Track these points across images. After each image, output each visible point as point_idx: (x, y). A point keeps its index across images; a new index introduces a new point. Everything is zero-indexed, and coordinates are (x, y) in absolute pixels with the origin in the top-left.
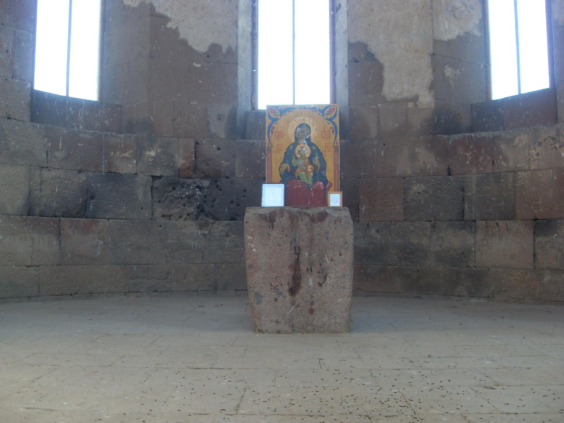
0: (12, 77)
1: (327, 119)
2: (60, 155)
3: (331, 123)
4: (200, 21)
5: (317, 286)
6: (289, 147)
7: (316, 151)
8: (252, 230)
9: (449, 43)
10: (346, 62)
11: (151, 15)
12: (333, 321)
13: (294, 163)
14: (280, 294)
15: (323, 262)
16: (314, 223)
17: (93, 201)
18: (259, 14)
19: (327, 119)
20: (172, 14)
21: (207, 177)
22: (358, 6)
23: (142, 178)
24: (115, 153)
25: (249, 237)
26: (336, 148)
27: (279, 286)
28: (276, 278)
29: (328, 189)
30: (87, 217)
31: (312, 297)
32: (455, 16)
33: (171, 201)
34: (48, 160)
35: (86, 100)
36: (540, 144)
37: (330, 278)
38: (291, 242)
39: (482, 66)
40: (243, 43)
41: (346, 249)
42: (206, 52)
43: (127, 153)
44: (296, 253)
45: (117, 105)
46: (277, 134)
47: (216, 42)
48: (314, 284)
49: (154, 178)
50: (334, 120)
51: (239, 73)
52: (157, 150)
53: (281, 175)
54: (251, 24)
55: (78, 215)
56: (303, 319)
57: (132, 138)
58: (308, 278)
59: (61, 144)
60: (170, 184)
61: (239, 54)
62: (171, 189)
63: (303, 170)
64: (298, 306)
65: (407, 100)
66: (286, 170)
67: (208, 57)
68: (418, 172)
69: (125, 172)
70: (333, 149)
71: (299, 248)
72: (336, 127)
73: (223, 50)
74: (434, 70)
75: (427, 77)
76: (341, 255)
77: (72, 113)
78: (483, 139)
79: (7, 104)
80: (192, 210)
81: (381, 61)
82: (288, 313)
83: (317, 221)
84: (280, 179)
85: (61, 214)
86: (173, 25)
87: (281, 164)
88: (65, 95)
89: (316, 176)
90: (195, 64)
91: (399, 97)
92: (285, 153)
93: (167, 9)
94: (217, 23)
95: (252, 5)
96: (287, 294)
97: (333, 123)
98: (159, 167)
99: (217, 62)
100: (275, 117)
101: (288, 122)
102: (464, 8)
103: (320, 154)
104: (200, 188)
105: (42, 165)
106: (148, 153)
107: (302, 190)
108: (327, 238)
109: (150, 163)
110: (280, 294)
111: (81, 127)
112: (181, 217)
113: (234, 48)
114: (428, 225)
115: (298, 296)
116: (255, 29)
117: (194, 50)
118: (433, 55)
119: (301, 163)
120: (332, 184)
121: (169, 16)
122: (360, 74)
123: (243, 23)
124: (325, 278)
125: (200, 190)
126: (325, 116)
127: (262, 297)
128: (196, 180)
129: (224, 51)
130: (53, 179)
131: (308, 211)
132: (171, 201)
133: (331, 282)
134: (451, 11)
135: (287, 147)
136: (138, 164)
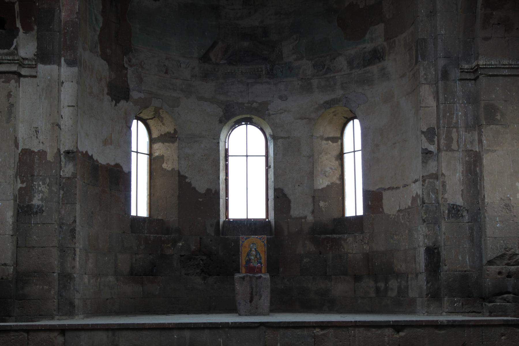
0: (125, 214)
1: (262, 241)
2: (142, 247)
4: (201, 177)
6: (248, 252)
9: (323, 189)
10: (273, 197)
12: (264, 311)
19: (262, 241)
22: (279, 170)
25: (237, 284)
26: (265, 252)
32: (326, 176)
36: (357, 242)
39: (340, 198)
40: (222, 186)
42: (204, 193)
49: (181, 256)
53: (245, 262)
54: (225, 174)
65: (301, 218)
66: (247, 260)
67: (205, 195)
70: (264, 252)
72: (265, 244)
75: (311, 208)
76: (266, 290)
77: (142, 225)
78: (334, 238)
80: (198, 271)
81: (290, 198)
90: (199, 199)
91: (298, 216)
96: (249, 302)
100: (243, 241)
102: (331, 171)
106: (178, 244)
108: (262, 284)
110: (247, 302)
112: (193, 274)
113: (218, 191)
121: (187, 176)
124: (261, 297)
125: (202, 261)
129: (213, 192)
131: (255, 275)
134: (324, 174)
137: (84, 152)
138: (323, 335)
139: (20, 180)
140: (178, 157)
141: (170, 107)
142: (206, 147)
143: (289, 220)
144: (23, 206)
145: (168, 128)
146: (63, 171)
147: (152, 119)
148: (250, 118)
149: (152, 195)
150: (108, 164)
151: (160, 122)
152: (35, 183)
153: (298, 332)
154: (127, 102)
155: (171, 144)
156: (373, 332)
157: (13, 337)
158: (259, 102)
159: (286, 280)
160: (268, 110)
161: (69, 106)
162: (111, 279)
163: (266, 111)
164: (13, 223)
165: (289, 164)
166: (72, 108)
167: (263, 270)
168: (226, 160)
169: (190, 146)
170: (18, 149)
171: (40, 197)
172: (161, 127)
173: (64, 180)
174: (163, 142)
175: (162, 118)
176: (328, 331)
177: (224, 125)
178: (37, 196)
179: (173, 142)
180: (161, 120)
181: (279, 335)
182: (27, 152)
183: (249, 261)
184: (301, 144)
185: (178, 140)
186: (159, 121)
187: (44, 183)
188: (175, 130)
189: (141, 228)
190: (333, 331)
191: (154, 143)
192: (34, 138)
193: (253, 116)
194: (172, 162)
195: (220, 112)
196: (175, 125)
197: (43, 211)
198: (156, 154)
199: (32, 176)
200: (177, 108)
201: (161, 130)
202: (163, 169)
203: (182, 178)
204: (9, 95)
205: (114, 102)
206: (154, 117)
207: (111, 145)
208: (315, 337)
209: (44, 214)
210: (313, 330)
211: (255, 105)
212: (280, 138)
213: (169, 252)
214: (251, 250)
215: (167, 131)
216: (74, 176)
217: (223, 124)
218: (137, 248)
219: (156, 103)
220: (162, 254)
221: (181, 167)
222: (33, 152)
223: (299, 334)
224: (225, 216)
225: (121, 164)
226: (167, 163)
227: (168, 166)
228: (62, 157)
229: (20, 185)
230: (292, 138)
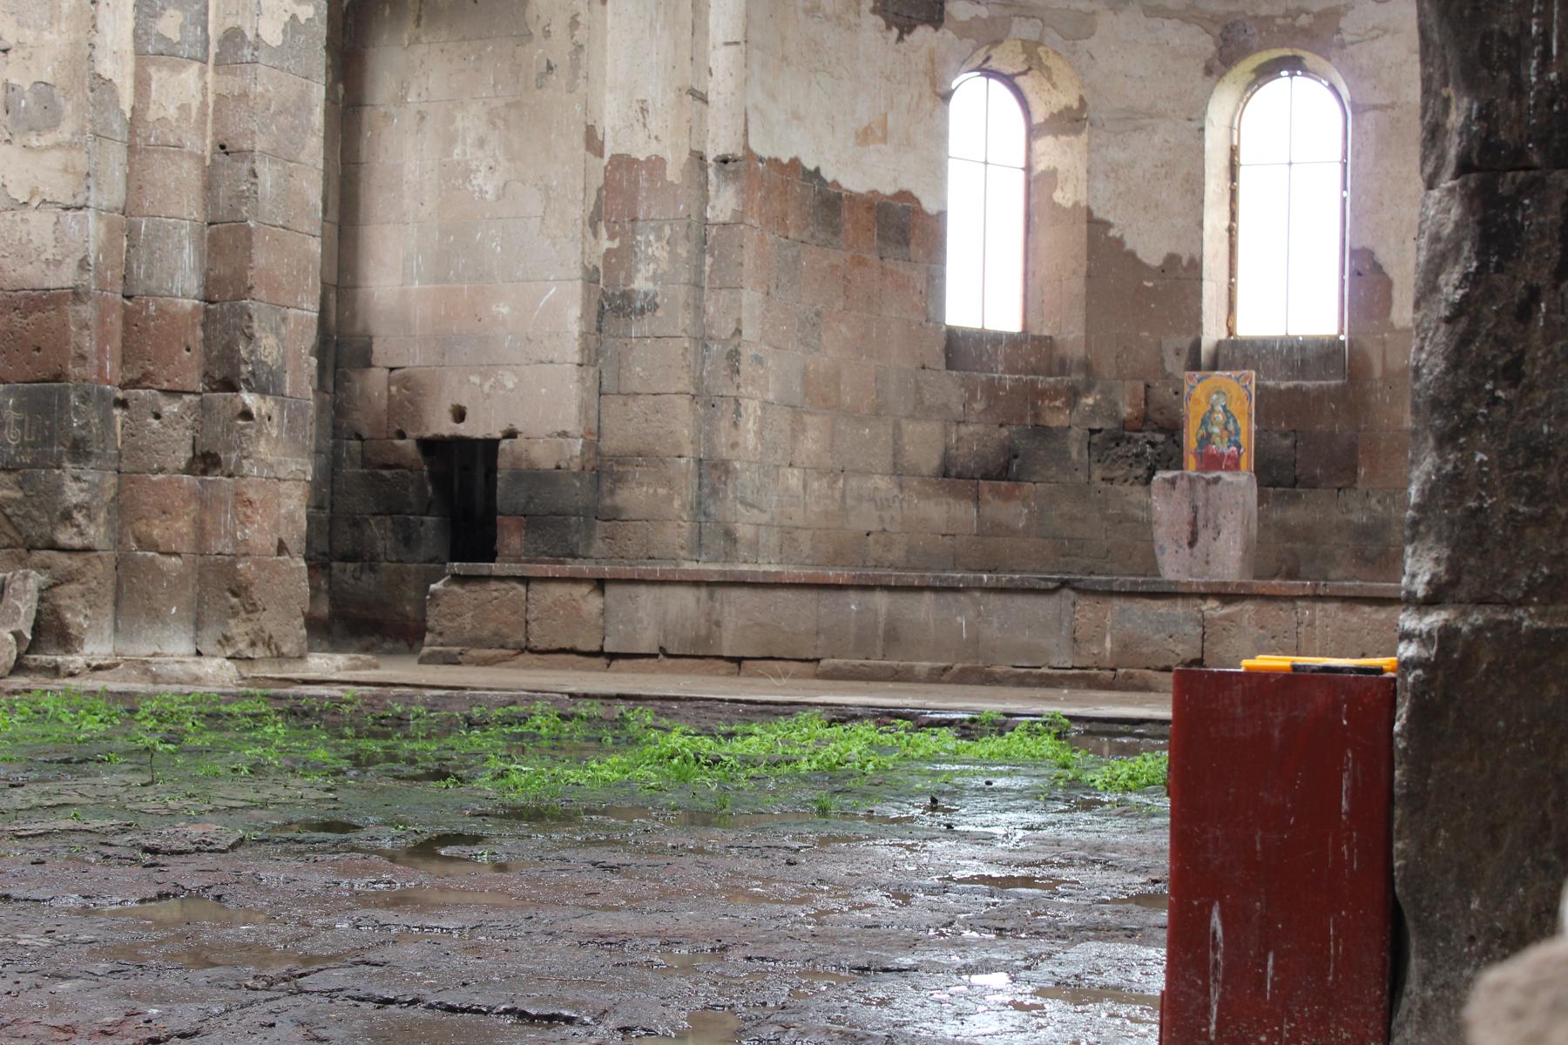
2: (979, 406)
21: (1161, 430)
23: (1076, 432)
33: (1113, 460)
47: (1175, 251)
49: (1092, 432)
54: (1227, 214)
55: (999, 477)
60: (1112, 440)
62: (1113, 445)
90: (1146, 283)
93: (1108, 212)
96: (1186, 547)
104: (1153, 444)
112: (1126, 481)
113: (1197, 259)
115: (1195, 549)
121: (1112, 220)
123: (1214, 219)
128: (1147, 434)
129: (1185, 262)
132: (1113, 460)
137: (785, 160)
138: (1227, 618)
139: (608, 230)
140: (1088, 172)
142: (1167, 141)
143: (1386, 335)
144: (613, 294)
146: (713, 208)
147: (1024, 73)
149: (1030, 275)
150: (874, 192)
152: (639, 238)
153: (1161, 607)
154: (936, 29)
155: (1073, 138)
157: (495, 594)
158: (1316, 9)
159: (1374, 501)
160: (1339, 31)
161: (727, 44)
162: (882, 483)
163: (1335, 37)
164: (583, 335)
166: (734, 48)
167: (1243, 463)
168: (1233, 177)
170: (600, 153)
171: (651, 273)
173: (714, 231)
174: (1056, 133)
175: (1048, 69)
178: (643, 271)
179: (1077, 132)
181: (1109, 615)
182: (624, 163)
183: (1206, 439)
187: (659, 239)
188: (1081, 99)
189: (984, 359)
191: (1036, 137)
192: (638, 127)
193: (1300, 53)
195: (1206, 44)
197: (657, 306)
198: (1040, 167)
199: (634, 220)
200: (1086, 41)
202: (1055, 206)
203: (1096, 227)
204: (574, 23)
205: (895, 31)
206: (1030, 69)
208: (1203, 623)
209: (659, 313)
211: (1304, 20)
213: (1056, 420)
214: (1212, 411)
216: (739, 219)
217: (1215, 77)
219: (1024, 29)
222: (636, 161)
223: (1161, 615)
224: (1225, 328)
225: (917, 193)
228: (711, 171)
229: (606, 244)
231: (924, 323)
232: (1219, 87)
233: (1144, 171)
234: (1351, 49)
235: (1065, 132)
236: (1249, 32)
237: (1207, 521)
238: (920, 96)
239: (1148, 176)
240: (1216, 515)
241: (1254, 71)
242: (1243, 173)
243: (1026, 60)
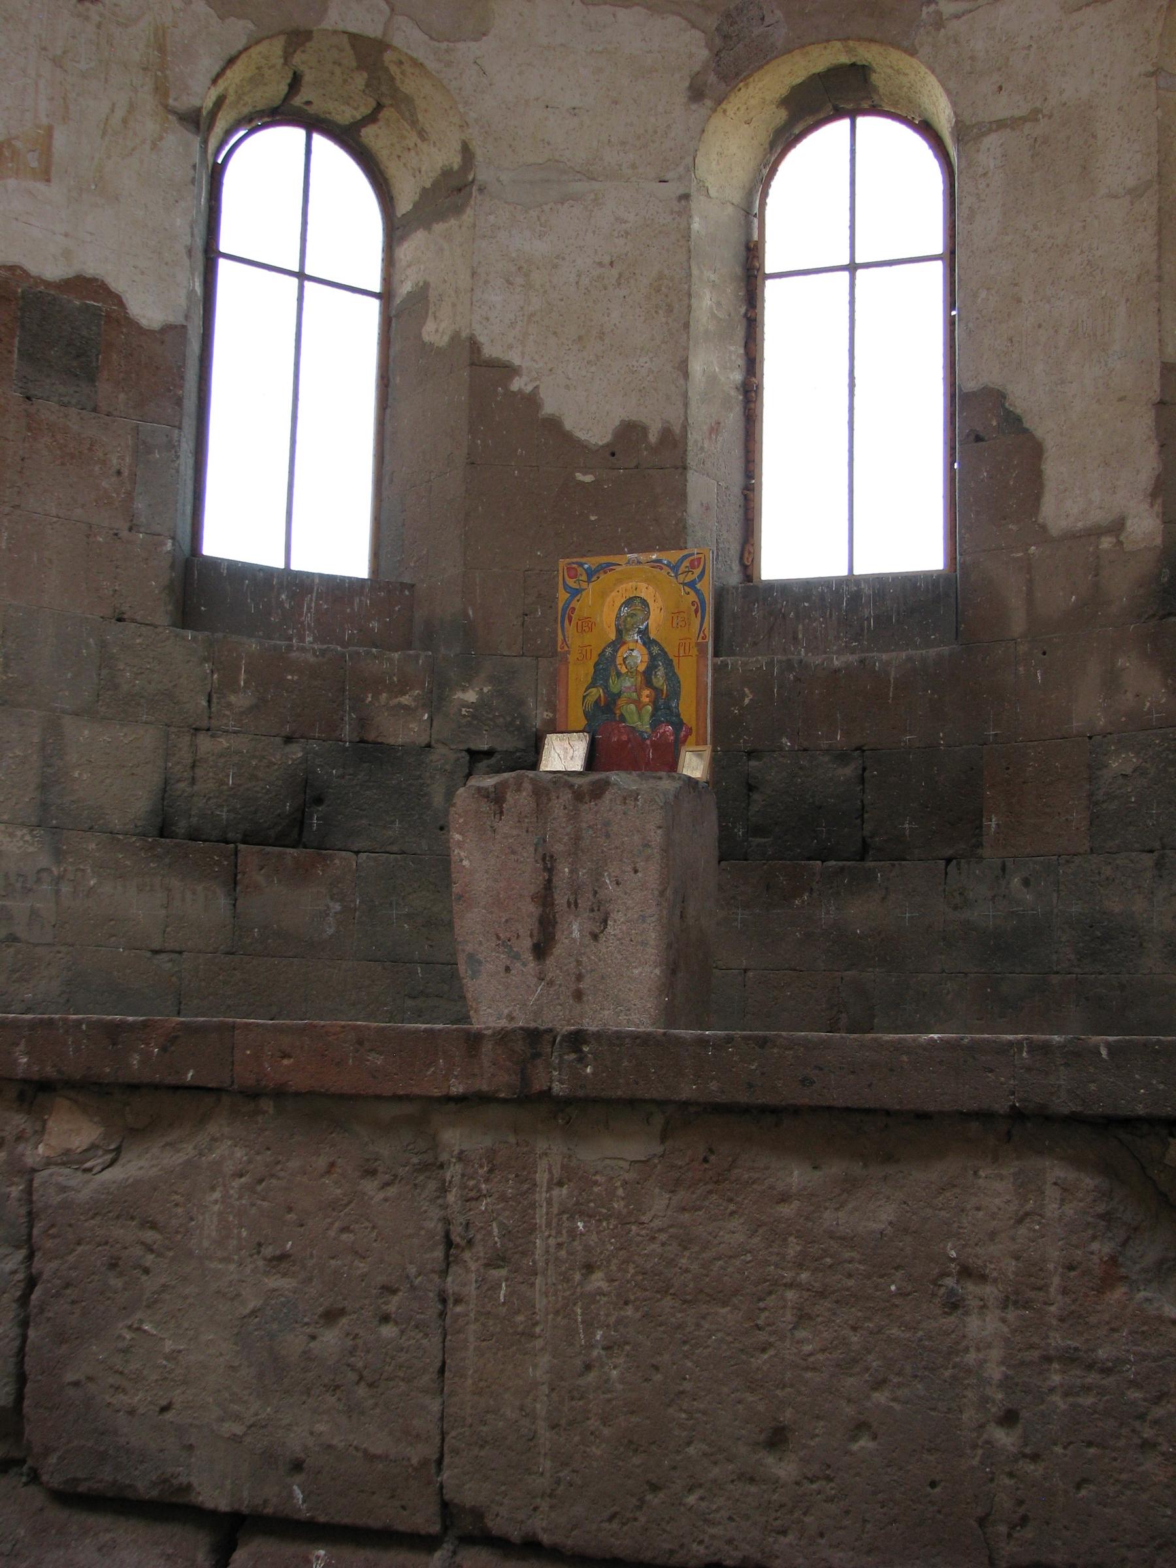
0: (130, 529)
1: (684, 584)
2: (241, 700)
3: (692, 593)
4: (593, 369)
5: (588, 940)
6: (604, 651)
7: (658, 656)
8: (461, 821)
11: (472, 364)
13: (614, 685)
14: (516, 957)
15: (599, 887)
16: (581, 802)
17: (320, 809)
18: (766, 336)
19: (684, 584)
20: (523, 358)
22: (983, 294)
24: (376, 696)
25: (458, 837)
27: (513, 940)
28: (507, 921)
29: (684, 742)
30: (305, 847)
31: (579, 963)
34: (210, 713)
35: (321, 576)
37: (615, 921)
38: (536, 845)
41: (648, 859)
42: (607, 445)
43: (407, 697)
44: (545, 869)
45: (401, 583)
46: (580, 623)
48: (582, 936)
50: (698, 586)
51: (689, 490)
52: (482, 689)
53: (586, 714)
54: (741, 362)
56: (561, 1013)
57: (421, 661)
58: (571, 923)
59: (243, 676)
61: (690, 443)
63: (631, 701)
64: (551, 983)
65: (1095, 532)
66: (597, 702)
68: (1123, 719)
69: (400, 741)
70: (694, 651)
71: (552, 857)
72: (703, 602)
73: (650, 436)
74: (1162, 446)
76: (636, 871)
77: (287, 606)
79: (117, 588)
81: (1039, 433)
82: (533, 999)
83: (587, 798)
84: (583, 722)
85: (239, 836)
86: (526, 385)
87: (587, 689)
88: (281, 565)
89: (659, 713)
90: (579, 476)
91: (1080, 524)
92: (596, 665)
93: (510, 347)
94: (635, 369)
95: (745, 315)
97: (697, 592)
98: (487, 728)
99: (637, 467)
101: (604, 594)
103: (669, 664)
105: (198, 724)
106: (459, 695)
107: (630, 745)
108: (608, 836)
109: (464, 721)
110: (516, 957)
111: (309, 639)
113: (677, 430)
114: (1148, 860)
115: (550, 961)
116: (754, 375)
117: (579, 441)
118: (1161, 404)
119: (628, 684)
120: (691, 729)
121: (517, 361)
122: (987, 471)
124: (605, 922)
126: (681, 578)
127: (480, 963)
129: (653, 438)
130: (221, 755)
133: (618, 932)
135: (600, 651)
136: (435, 723)
141: (431, 38)
145: (440, 150)
147: (371, 118)
148: (853, 65)
151: (408, 128)
156: (787, 1210)
159: (1016, 881)
165: (1035, 251)
169: (539, 219)
172: (417, 154)
174: (428, 227)
175: (408, 100)
176: (188, 1151)
177: (714, 110)
179: (458, 210)
180: (407, 114)
184: (1094, 136)
185: (474, 194)
186: (405, 124)
190: (239, 1153)
191: (403, 238)
193: (867, 54)
194: (454, 305)
196: (461, 126)
198: (405, 288)
200: (471, 44)
201: (420, 172)
202: (426, 349)
206: (379, 107)
207: (48, 180)
210: (19, 1138)
212: (990, 131)
215: (440, 165)
217: (708, 103)
218: (209, 701)
220: (362, 741)
221: (487, 319)
224: (736, 567)
225: (118, 285)
226: (435, 318)
227: (441, 330)
230: (1050, 117)
231: (124, 534)
232: (717, 121)
233: (579, 276)
234: (954, 26)
235: (441, 216)
236: (768, 21)
237: (576, 890)
238: (132, 108)
239: (585, 281)
240: (597, 875)
241: (785, 102)
242: (772, 291)
243: (367, 86)
